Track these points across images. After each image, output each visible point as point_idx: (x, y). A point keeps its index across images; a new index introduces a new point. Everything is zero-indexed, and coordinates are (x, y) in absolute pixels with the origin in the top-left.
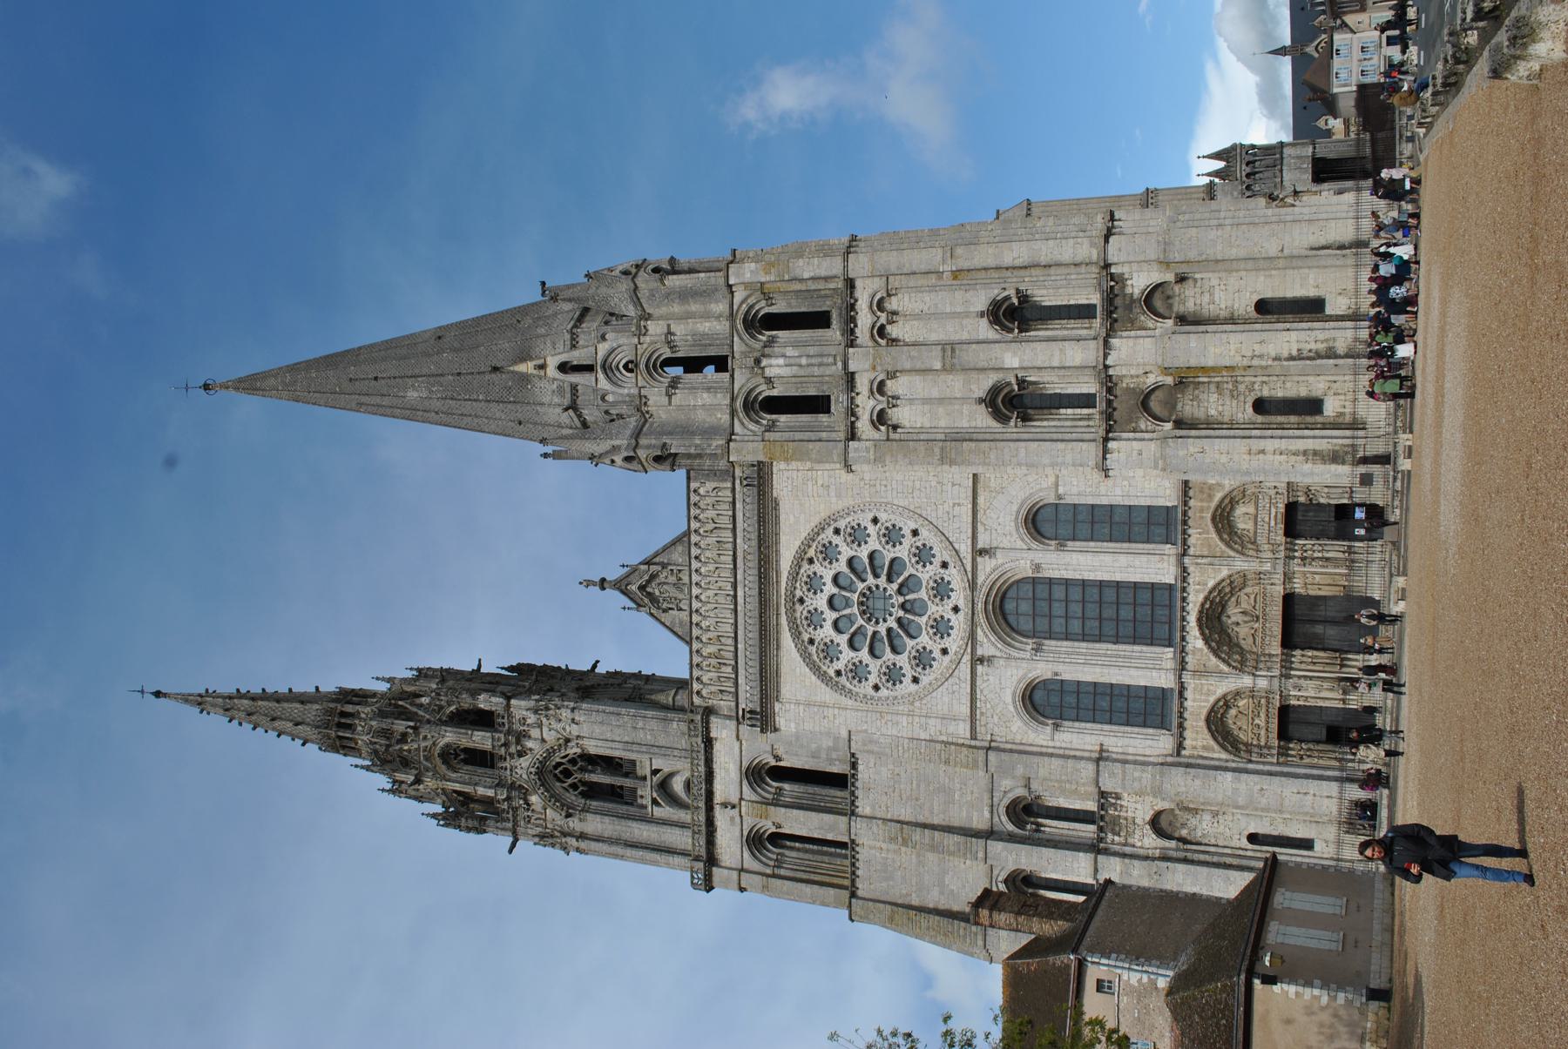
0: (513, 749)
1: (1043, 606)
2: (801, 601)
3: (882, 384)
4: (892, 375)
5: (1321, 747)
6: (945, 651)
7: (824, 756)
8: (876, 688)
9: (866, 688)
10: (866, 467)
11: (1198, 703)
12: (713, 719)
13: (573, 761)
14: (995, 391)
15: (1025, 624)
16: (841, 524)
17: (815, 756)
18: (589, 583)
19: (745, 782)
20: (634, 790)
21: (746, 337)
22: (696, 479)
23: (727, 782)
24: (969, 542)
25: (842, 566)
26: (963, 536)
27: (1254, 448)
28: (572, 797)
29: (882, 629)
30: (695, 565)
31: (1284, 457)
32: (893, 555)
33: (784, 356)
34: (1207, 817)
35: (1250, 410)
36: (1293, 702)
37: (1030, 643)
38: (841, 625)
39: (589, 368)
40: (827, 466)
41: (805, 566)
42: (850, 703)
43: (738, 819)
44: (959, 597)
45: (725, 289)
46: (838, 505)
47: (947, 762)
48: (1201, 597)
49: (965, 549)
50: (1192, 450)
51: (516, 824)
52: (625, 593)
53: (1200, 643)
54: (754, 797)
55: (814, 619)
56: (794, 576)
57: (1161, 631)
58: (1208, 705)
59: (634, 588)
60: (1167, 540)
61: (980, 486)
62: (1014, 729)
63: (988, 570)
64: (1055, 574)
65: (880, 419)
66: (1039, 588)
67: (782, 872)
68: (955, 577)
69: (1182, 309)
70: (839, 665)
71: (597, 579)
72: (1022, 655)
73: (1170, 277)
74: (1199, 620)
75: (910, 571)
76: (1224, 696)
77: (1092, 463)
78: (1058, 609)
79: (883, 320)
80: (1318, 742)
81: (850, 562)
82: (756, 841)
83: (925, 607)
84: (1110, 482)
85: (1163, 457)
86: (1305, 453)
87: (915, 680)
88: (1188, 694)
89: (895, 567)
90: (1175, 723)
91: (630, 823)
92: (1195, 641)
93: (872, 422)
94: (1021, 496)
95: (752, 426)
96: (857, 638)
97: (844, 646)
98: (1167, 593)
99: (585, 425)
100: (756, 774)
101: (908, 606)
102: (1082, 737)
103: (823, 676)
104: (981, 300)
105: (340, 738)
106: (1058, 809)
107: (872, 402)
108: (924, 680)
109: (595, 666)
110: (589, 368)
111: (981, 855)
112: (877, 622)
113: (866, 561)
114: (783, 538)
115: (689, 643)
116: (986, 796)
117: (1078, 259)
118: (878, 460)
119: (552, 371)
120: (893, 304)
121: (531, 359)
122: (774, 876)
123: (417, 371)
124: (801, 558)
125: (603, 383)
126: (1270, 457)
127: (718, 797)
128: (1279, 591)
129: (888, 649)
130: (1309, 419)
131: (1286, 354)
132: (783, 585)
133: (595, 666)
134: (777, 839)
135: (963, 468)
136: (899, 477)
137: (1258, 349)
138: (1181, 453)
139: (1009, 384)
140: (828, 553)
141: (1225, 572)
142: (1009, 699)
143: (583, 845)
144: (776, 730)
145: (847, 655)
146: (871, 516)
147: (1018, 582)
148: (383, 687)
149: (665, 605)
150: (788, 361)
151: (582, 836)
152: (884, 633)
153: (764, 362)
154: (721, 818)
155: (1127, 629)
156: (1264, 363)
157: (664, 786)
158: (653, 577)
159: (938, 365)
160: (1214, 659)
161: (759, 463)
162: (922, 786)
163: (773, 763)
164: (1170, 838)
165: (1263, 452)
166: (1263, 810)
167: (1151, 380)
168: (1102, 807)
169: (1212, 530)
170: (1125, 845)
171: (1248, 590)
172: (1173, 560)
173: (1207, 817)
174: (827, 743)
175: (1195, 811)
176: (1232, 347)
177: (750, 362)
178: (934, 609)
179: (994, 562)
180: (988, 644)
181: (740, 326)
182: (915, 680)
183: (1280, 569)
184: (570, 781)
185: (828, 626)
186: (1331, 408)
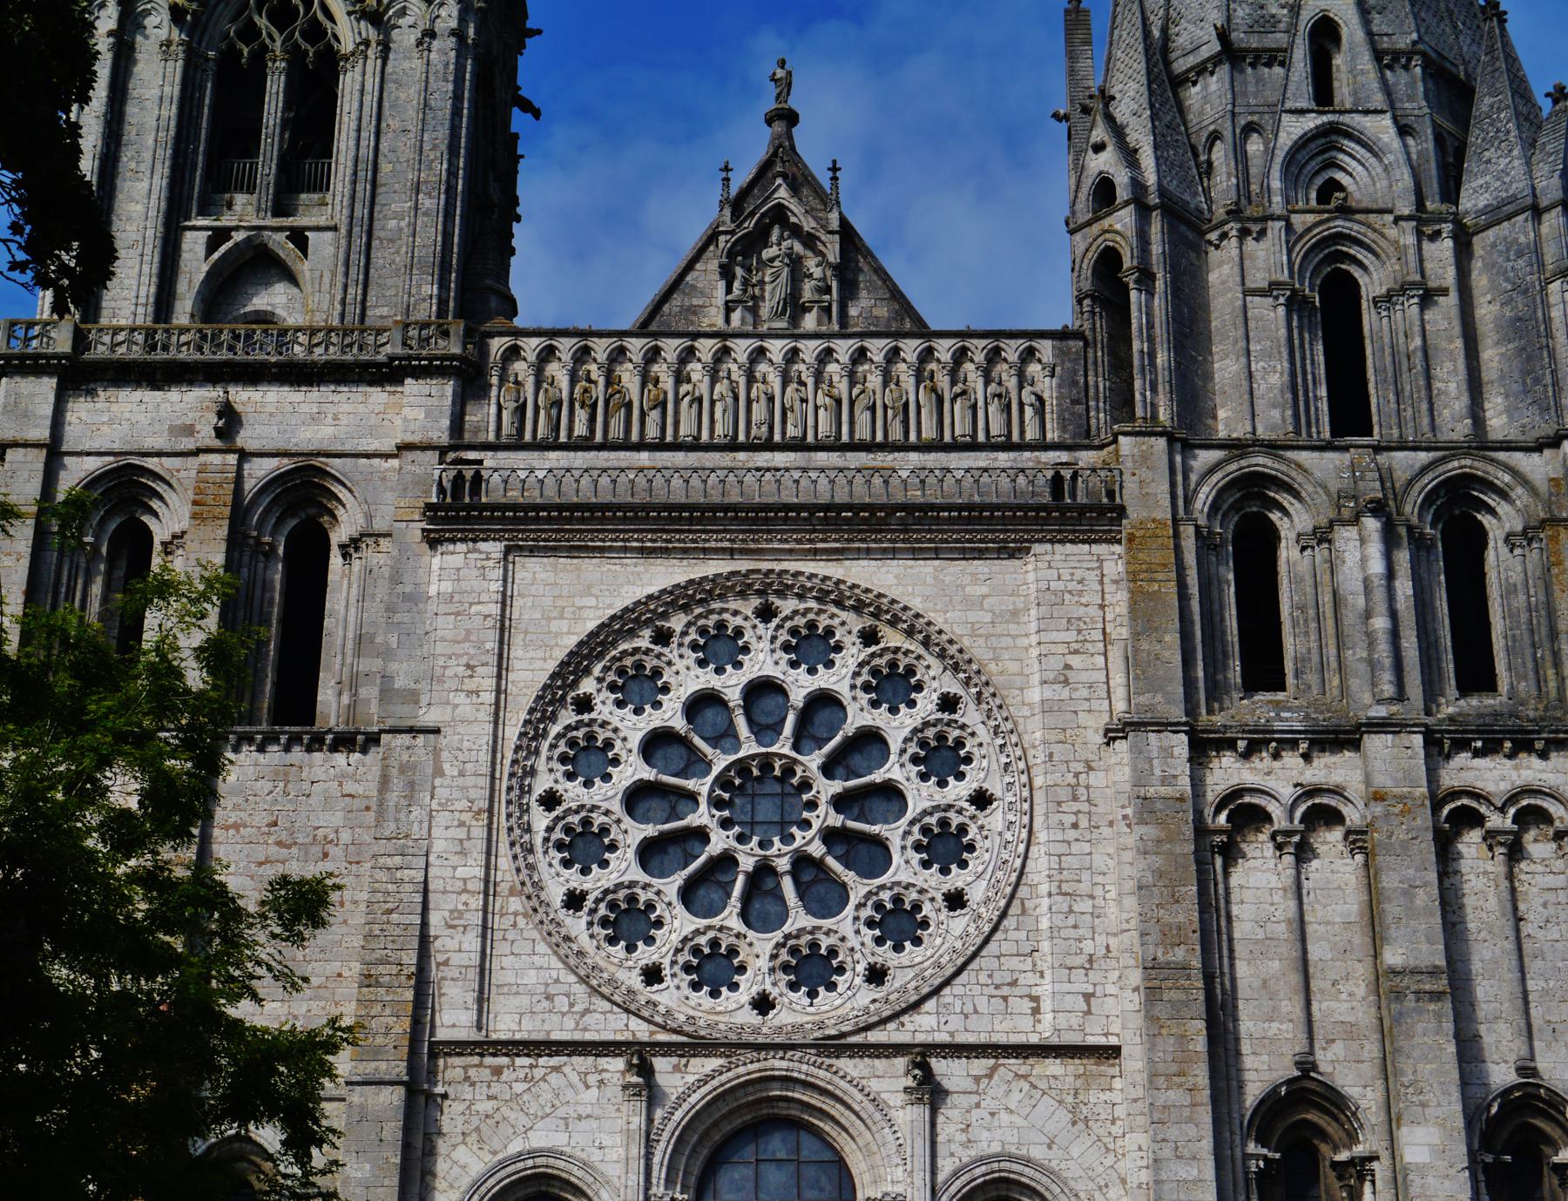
3: (1332, 817)
4: (1357, 840)
7: (367, 664)
10: (1123, 775)
14: (1335, 1102)
16: (970, 714)
19: (286, 464)
21: (1429, 481)
22: (1060, 354)
23: (282, 419)
24: (942, 1037)
25: (860, 715)
26: (956, 1022)
29: (702, 816)
39: (1323, 93)
40: (1118, 679)
41: (856, 623)
42: (512, 732)
43: (187, 444)
44: (796, 1012)
47: (368, 981)
49: (924, 1027)
52: (765, 169)
54: (250, 485)
55: (720, 646)
61: (1089, 1065)
62: (461, 1154)
63: (874, 1085)
65: (1247, 814)
70: (605, 707)
71: (793, 103)
75: (858, 887)
79: (1495, 821)
83: (766, 926)
89: (863, 849)
93: (1237, 793)
97: (653, 719)
100: (305, 490)
107: (1287, 793)
108: (577, 924)
110: (1323, 93)
112: (717, 803)
113: (877, 777)
114: (926, 569)
124: (878, 612)
125: (1294, 128)
127: (242, 396)
129: (650, 830)
135: (1137, 1021)
139: (1352, 1139)
140: (892, 685)
142: (538, 1140)
144: (433, 541)
145: (632, 727)
146: (995, 787)
150: (1378, 584)
154: (192, 405)
158: (810, 241)
159: (1393, 957)
161: (1121, 511)
179: (897, 1099)
181: (1454, 466)
182: (574, 901)
185: (705, 679)
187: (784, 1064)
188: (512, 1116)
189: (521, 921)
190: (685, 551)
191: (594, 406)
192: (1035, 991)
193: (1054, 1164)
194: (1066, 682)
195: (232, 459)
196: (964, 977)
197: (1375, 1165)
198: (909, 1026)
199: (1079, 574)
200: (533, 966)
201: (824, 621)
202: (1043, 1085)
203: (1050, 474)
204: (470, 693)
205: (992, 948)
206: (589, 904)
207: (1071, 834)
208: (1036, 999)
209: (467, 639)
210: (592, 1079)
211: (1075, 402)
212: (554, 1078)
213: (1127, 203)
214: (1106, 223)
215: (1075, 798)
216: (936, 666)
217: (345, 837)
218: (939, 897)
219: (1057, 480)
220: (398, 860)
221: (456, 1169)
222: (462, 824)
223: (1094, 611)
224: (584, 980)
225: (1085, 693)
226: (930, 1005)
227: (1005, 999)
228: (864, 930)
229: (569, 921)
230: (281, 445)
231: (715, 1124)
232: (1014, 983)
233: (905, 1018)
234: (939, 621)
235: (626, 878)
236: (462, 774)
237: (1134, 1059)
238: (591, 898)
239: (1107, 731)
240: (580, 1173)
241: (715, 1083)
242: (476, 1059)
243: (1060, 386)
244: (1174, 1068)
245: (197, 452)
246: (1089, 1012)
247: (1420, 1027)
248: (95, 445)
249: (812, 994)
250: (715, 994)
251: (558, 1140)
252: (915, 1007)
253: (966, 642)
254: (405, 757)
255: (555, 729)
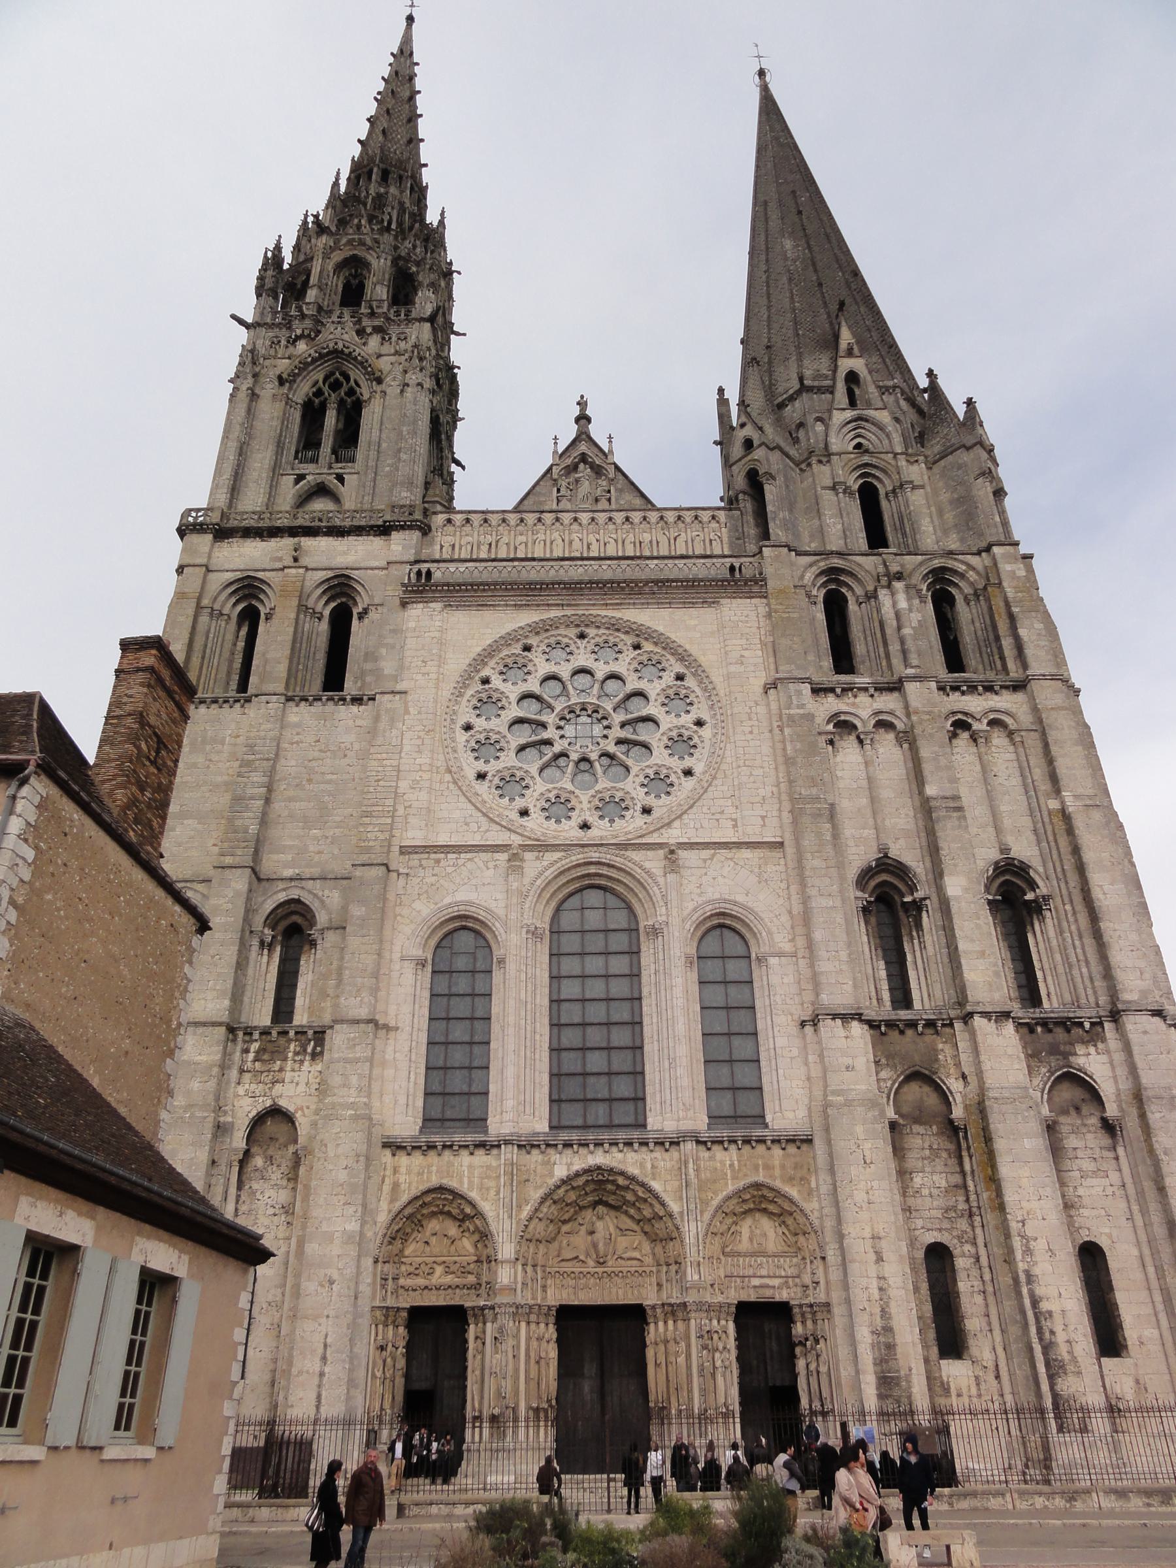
0: (366, 322)
1: (596, 943)
2: (582, 636)
5: (400, 1382)
6: (524, 813)
7: (368, 666)
8: (468, 727)
9: (466, 714)
10: (774, 706)
11: (466, 1172)
12: (416, 535)
13: (351, 392)
14: (900, 870)
15: (569, 919)
16: (690, 682)
17: (371, 656)
18: (582, 404)
19: (330, 574)
20: (314, 460)
21: (924, 570)
22: (727, 517)
23: (329, 554)
27: (884, 1244)
28: (303, 390)
29: (550, 733)
30: (619, 517)
31: (876, 1294)
32: (654, 744)
33: (910, 610)
34: (283, 1196)
35: (931, 1238)
36: (472, 1331)
37: (544, 924)
38: (552, 683)
43: (279, 565)
44: (601, 830)
45: (984, 544)
46: (717, 676)
48: (634, 1171)
49: (673, 835)
50: (867, 1145)
51: (271, 326)
53: (561, 1172)
56: (615, 626)
57: (573, 1115)
58: (464, 1188)
59: (583, 447)
60: (714, 1118)
62: (417, 905)
63: (647, 865)
64: (646, 958)
65: (844, 726)
66: (623, 938)
67: (204, 619)
68: (633, 824)
69: (1064, 1129)
70: (496, 682)
72: (527, 914)
73: (1111, 1110)
74: (599, 1168)
76: (479, 1214)
77: (825, 998)
78: (595, 965)
80: (407, 1376)
81: (640, 694)
82: (249, 589)
83: (585, 787)
84: (794, 1029)
85: (848, 1103)
86: (888, 1330)
87: (481, 776)
88: (480, 1158)
90: (437, 1139)
91: (272, 448)
92: (564, 1165)
93: (837, 715)
94: (758, 907)
95: (809, 576)
96: (535, 705)
97: (523, 688)
98: (630, 1120)
99: (781, 406)
101: (584, 766)
102: (407, 1001)
103: (481, 660)
104: (1024, 849)
105: (370, 173)
106: (295, 973)
107: (865, 713)
108: (482, 788)
109: (458, 463)
110: (853, 403)
111: (228, 860)
113: (644, 713)
114: (665, 613)
115: (517, 510)
116: (316, 871)
117: (1119, 974)
118: (784, 721)
119: (846, 364)
120: (999, 739)
121: (858, 342)
122: (199, 608)
123: (816, 249)
126: (873, 1271)
127: (307, 542)
128: (649, 1297)
129: (523, 741)
130: (932, 1334)
131: (1039, 1291)
132: (603, 613)
133: (458, 463)
134: (250, 618)
136: (766, 749)
137: (1039, 1246)
138: (859, 1129)
139: (912, 889)
141: (674, 1207)
142: (461, 896)
143: (243, 395)
144: (404, 604)
145: (512, 691)
146: (705, 716)
147: (629, 908)
148: (432, 218)
149: (563, 483)
151: (254, 396)
152: (545, 735)
153: (899, 585)
155: (571, 1062)
156: (1019, 1255)
157: (321, 490)
160: (536, 1195)
162: (329, 787)
163: (355, 612)
164: (250, 1138)
165: (880, 1259)
166: (297, 1287)
167: (954, 1085)
168: (300, 1033)
169: (741, 1184)
170: (242, 1071)
171: (647, 1247)
172: (687, 1125)
173: (283, 1196)
174: (388, 667)
175: (293, 1177)
176: (1035, 1205)
177: (894, 568)
178: (584, 802)
180: (538, 868)
181: (937, 563)
183: (691, 1298)
184: (326, 389)
185: (550, 668)
186: (954, 1371)
187: (597, 855)
188: (446, 884)
189: (452, 786)
190: (538, 605)
191: (490, 545)
192: (734, 816)
193: (750, 904)
194: (742, 663)
195: (301, 571)
196: (694, 809)
197: (928, 902)
198: (666, 835)
199: (745, 613)
200: (457, 808)
201: (612, 640)
202: (742, 863)
203: (728, 565)
204: (424, 674)
205: (709, 794)
206: (489, 777)
207: (749, 737)
208: (735, 820)
209: (423, 649)
210: (491, 865)
211: (738, 539)
212: (469, 865)
213: (760, 445)
214: (749, 458)
215: (750, 719)
216: (672, 660)
217: (356, 746)
218: (679, 772)
219: (732, 569)
220: (384, 756)
221: (414, 913)
222: (419, 737)
223: (754, 630)
224: (485, 815)
225: (753, 668)
226: (677, 824)
227: (718, 820)
228: (639, 788)
229: (477, 787)
230: (326, 564)
231: (559, 888)
232: (722, 812)
233: (663, 831)
234: (673, 637)
235: (509, 765)
236: (419, 713)
237: (790, 850)
238: (489, 775)
239: (766, 684)
240: (484, 914)
241: (559, 865)
242: (426, 856)
243: (730, 531)
244: (816, 848)
245: (282, 569)
246: (764, 825)
247: (949, 825)
248: (231, 567)
249: (612, 821)
250: (558, 821)
251: (472, 897)
252: (669, 824)
253: (687, 647)
254: (389, 706)
255: (470, 692)
